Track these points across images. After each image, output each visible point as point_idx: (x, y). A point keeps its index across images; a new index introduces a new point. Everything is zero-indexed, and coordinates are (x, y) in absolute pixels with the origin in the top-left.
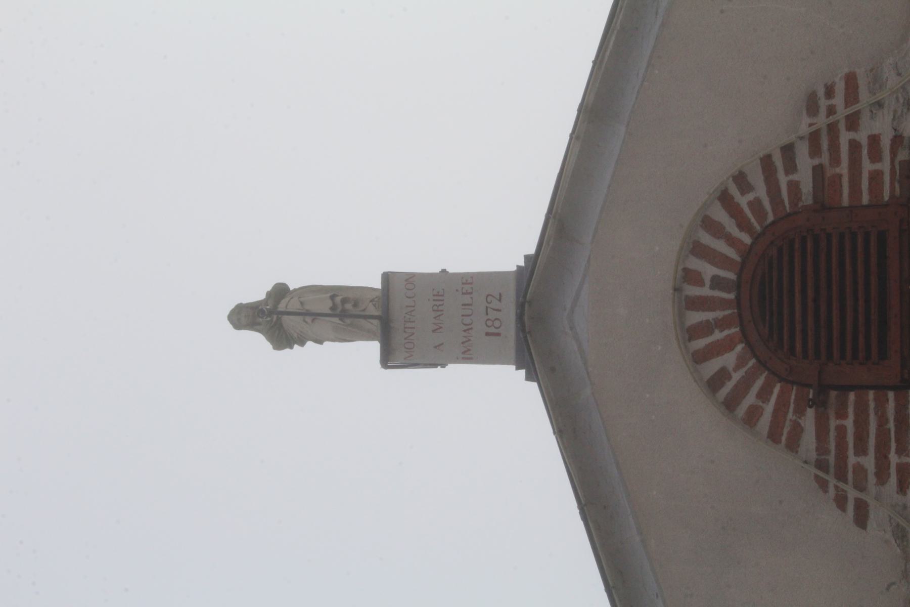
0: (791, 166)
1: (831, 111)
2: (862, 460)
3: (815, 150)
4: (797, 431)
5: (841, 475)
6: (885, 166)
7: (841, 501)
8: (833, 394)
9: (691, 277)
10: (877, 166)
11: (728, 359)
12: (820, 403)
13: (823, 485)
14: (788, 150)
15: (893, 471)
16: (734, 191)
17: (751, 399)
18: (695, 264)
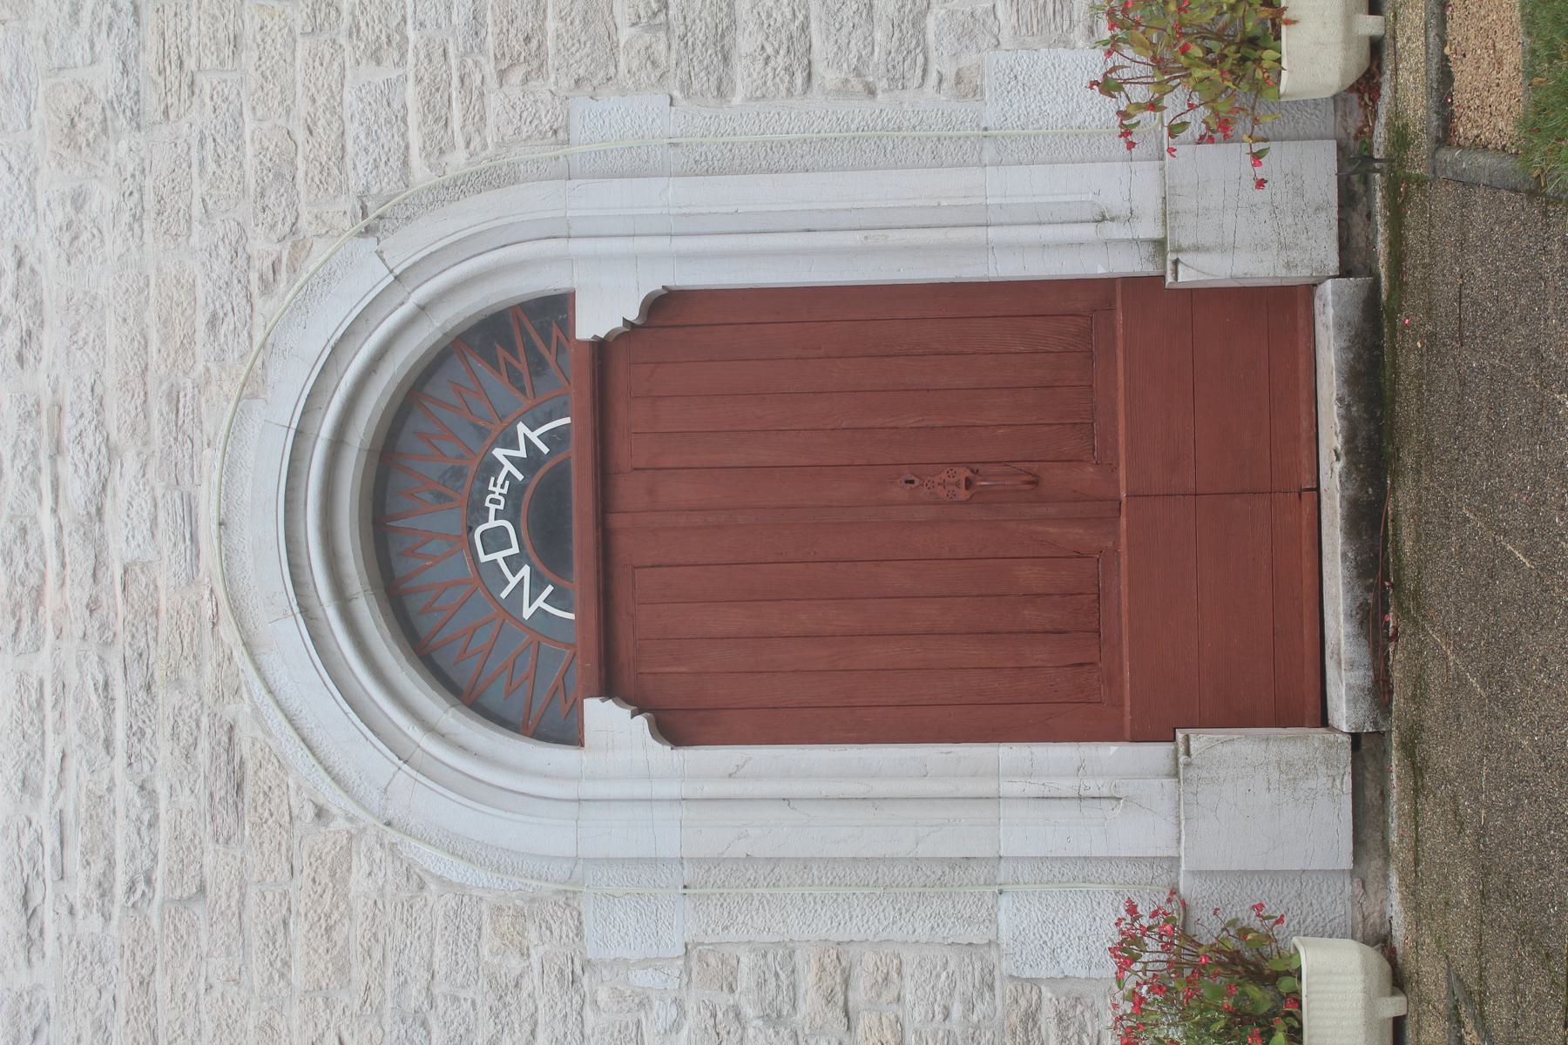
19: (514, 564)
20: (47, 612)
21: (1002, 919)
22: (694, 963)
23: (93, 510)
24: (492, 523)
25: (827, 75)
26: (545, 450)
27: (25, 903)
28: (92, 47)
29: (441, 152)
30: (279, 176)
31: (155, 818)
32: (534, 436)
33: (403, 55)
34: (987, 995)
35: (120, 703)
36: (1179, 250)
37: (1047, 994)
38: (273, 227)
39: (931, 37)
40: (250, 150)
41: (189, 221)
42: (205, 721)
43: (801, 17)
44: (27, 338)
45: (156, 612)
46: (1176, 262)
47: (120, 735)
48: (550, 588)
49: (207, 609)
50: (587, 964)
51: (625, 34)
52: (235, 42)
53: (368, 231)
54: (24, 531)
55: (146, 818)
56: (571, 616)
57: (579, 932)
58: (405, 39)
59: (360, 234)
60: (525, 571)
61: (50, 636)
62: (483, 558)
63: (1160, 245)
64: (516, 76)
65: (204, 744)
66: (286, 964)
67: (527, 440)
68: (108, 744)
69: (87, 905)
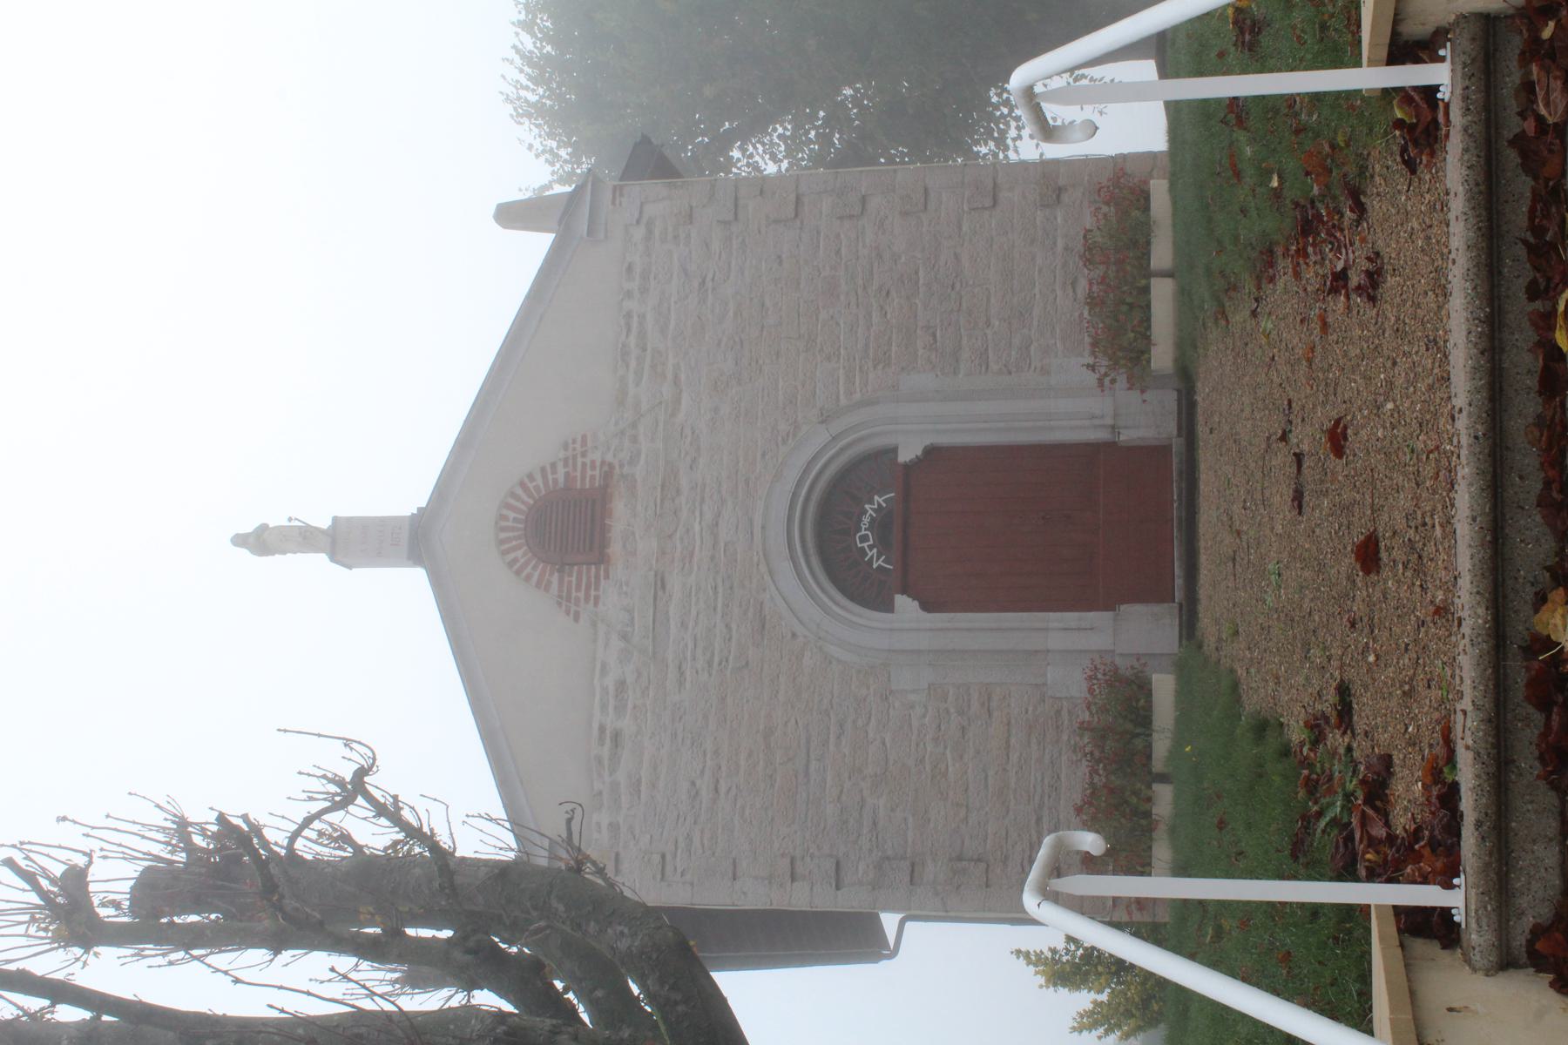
0: (554, 471)
1: (574, 449)
2: (578, 594)
3: (566, 464)
4: (549, 583)
5: (569, 600)
6: (597, 472)
7: (568, 613)
8: (567, 567)
9: (504, 517)
10: (594, 473)
11: (519, 553)
12: (561, 571)
13: (560, 604)
14: (553, 466)
15: (592, 598)
16: (526, 480)
17: (529, 569)
18: (505, 512)
19: (871, 548)
20: (696, 559)
21: (1049, 675)
22: (932, 692)
23: (714, 522)
24: (863, 532)
25: (994, 367)
26: (884, 505)
27: (680, 668)
28: (725, 356)
29: (851, 394)
30: (791, 402)
31: (730, 640)
32: (880, 500)
33: (839, 358)
34: (1042, 705)
35: (720, 595)
36: (1119, 428)
37: (1065, 703)
38: (787, 420)
39: (1032, 353)
40: (780, 393)
41: (757, 419)
42: (752, 601)
43: (985, 346)
44: (694, 460)
45: (736, 561)
46: (1119, 433)
47: (720, 605)
48: (883, 557)
49: (755, 559)
50: (891, 692)
51: (920, 352)
52: (778, 354)
53: (822, 422)
54: (688, 531)
55: (727, 637)
56: (891, 567)
57: (889, 680)
58: (840, 354)
59: (819, 423)
60: (875, 550)
61: (695, 568)
62: (859, 545)
63: (1113, 427)
64: (880, 367)
65: (751, 610)
66: (777, 692)
67: (879, 504)
68: (715, 609)
69: (703, 670)
